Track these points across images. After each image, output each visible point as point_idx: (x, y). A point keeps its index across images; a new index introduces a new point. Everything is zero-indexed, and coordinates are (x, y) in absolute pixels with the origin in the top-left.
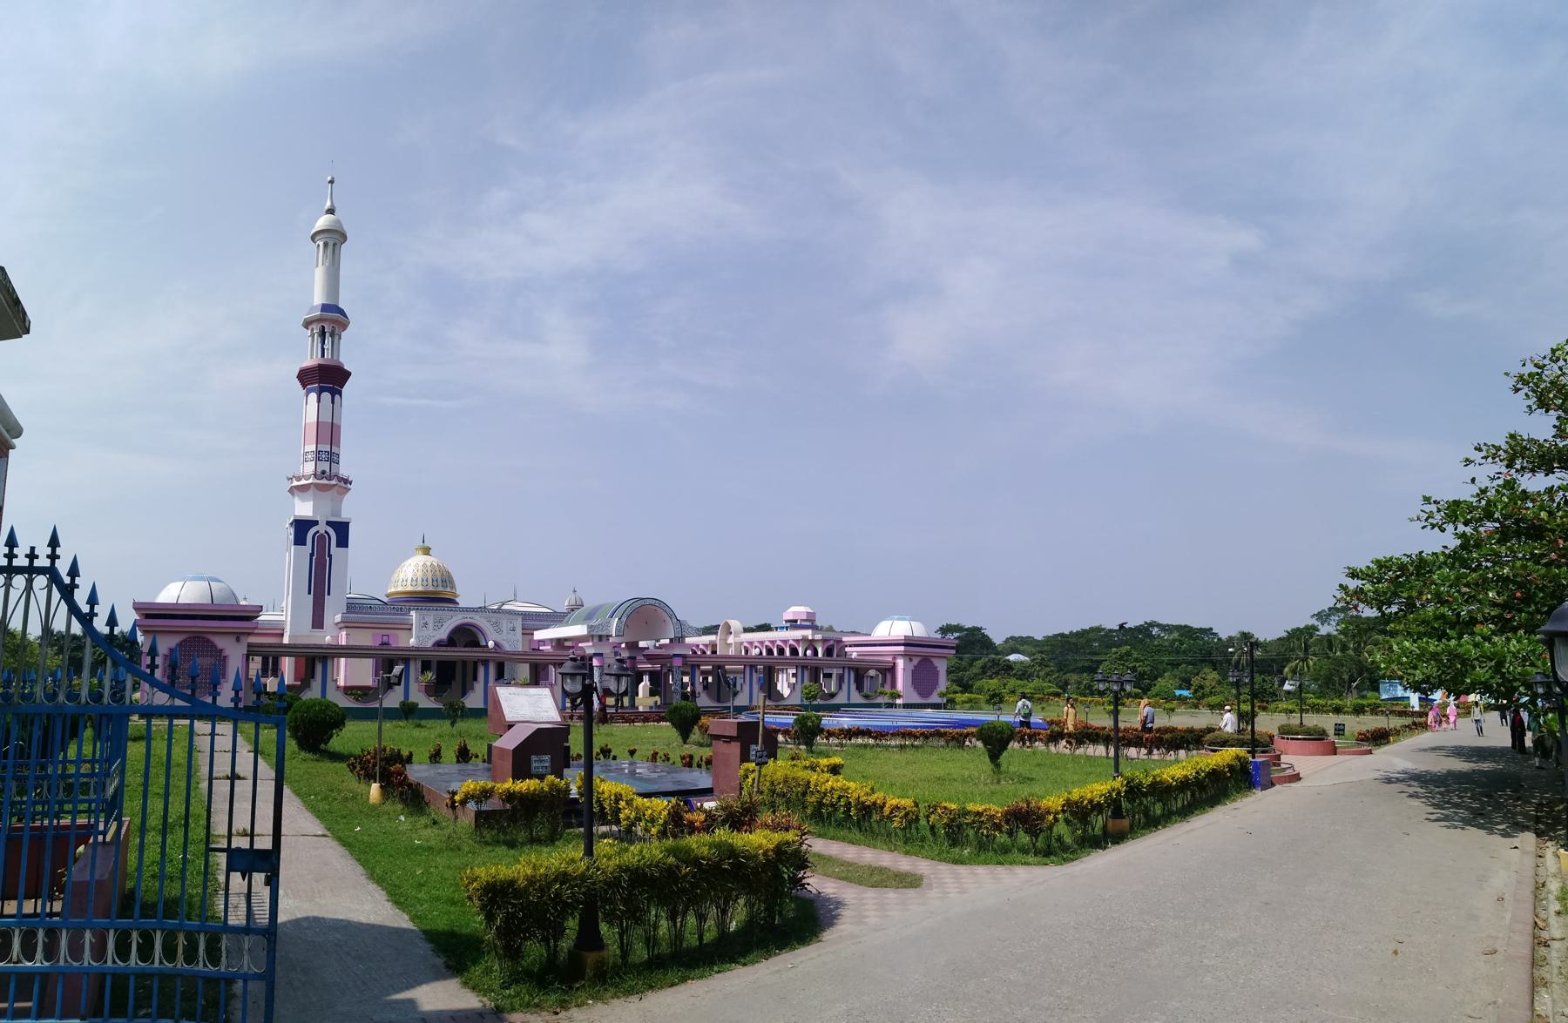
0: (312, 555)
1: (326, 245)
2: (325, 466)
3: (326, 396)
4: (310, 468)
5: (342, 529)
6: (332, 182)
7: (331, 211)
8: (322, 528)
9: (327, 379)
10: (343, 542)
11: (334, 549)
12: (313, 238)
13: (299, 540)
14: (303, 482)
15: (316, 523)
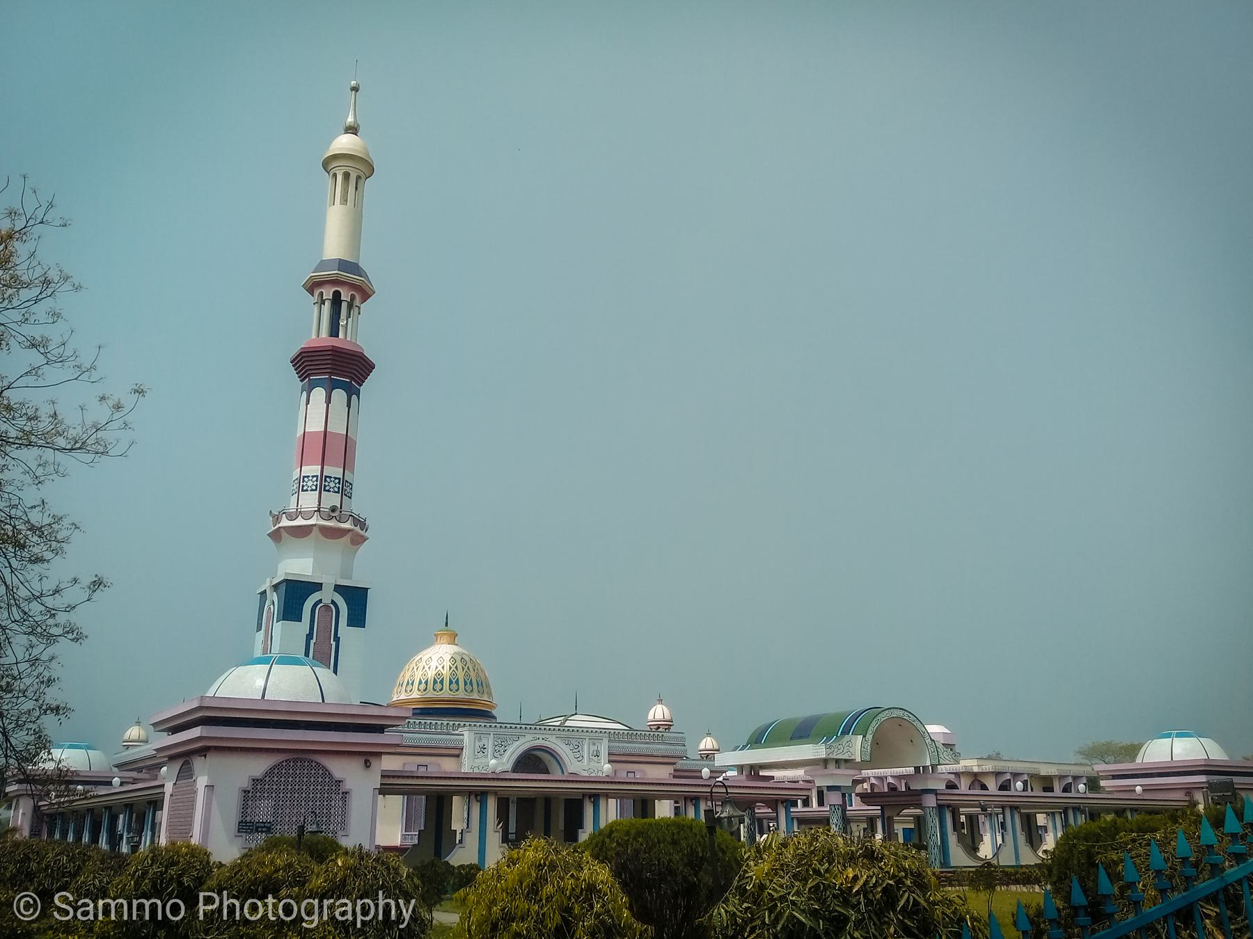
0: (309, 637)
1: (347, 176)
2: (332, 499)
3: (339, 395)
4: (309, 500)
5: (356, 599)
6: (355, 89)
7: (353, 130)
8: (327, 595)
9: (337, 368)
10: (358, 618)
11: (344, 630)
12: (326, 164)
13: (291, 612)
14: (300, 522)
15: (318, 587)
